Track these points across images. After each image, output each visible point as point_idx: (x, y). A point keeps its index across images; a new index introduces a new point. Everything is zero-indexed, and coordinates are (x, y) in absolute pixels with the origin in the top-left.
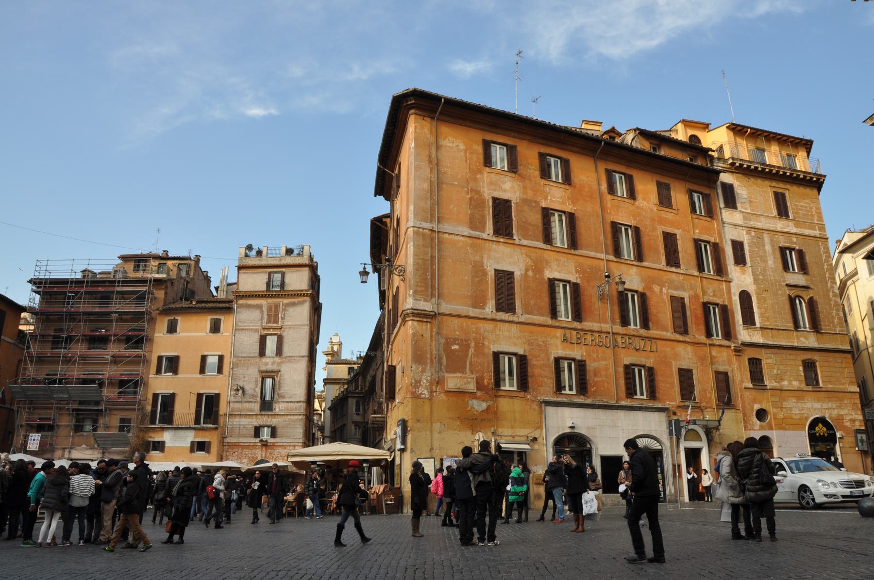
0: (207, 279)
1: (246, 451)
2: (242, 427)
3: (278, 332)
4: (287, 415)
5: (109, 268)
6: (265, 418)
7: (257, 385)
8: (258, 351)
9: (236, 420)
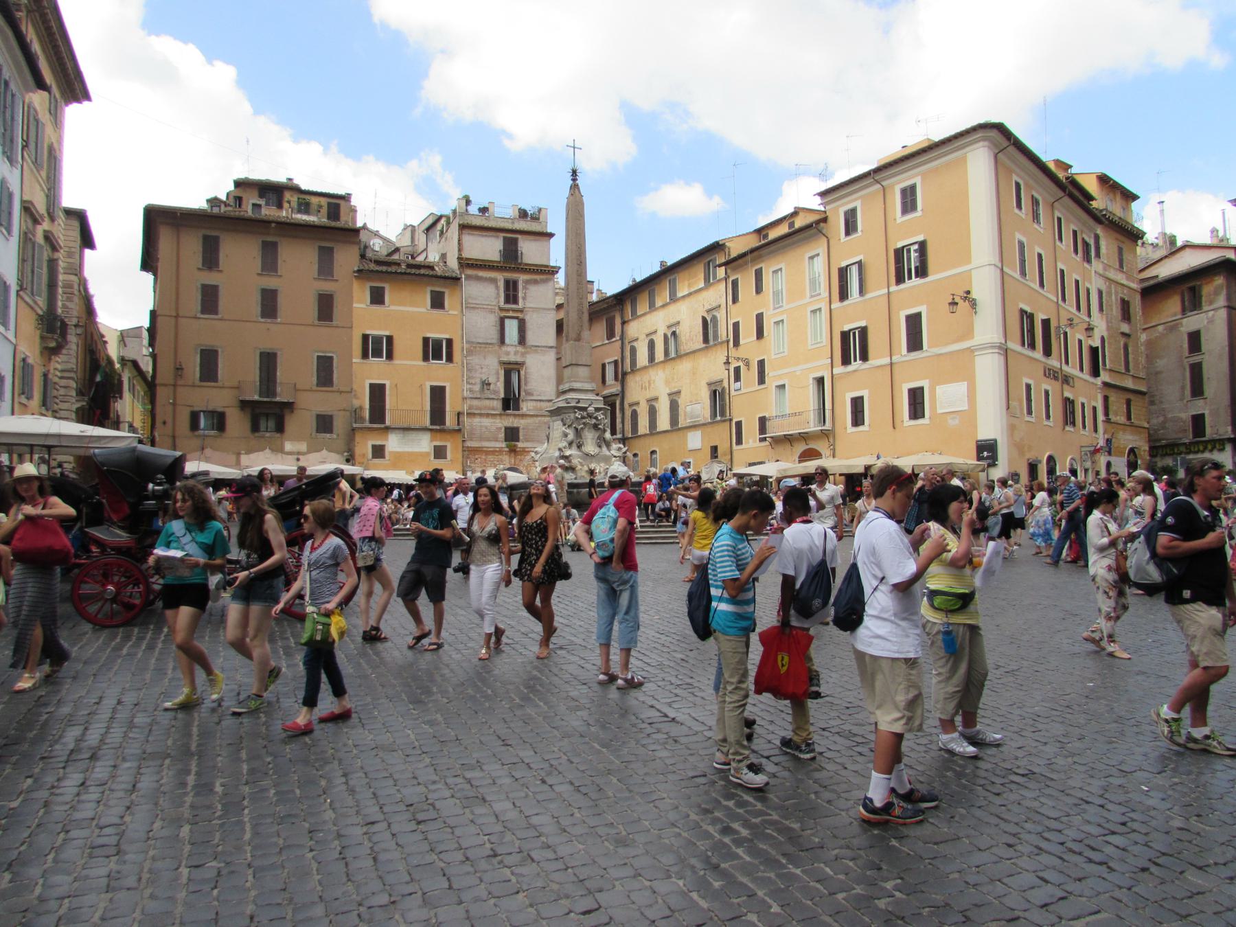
1: (490, 457)
4: (537, 416)
6: (511, 419)
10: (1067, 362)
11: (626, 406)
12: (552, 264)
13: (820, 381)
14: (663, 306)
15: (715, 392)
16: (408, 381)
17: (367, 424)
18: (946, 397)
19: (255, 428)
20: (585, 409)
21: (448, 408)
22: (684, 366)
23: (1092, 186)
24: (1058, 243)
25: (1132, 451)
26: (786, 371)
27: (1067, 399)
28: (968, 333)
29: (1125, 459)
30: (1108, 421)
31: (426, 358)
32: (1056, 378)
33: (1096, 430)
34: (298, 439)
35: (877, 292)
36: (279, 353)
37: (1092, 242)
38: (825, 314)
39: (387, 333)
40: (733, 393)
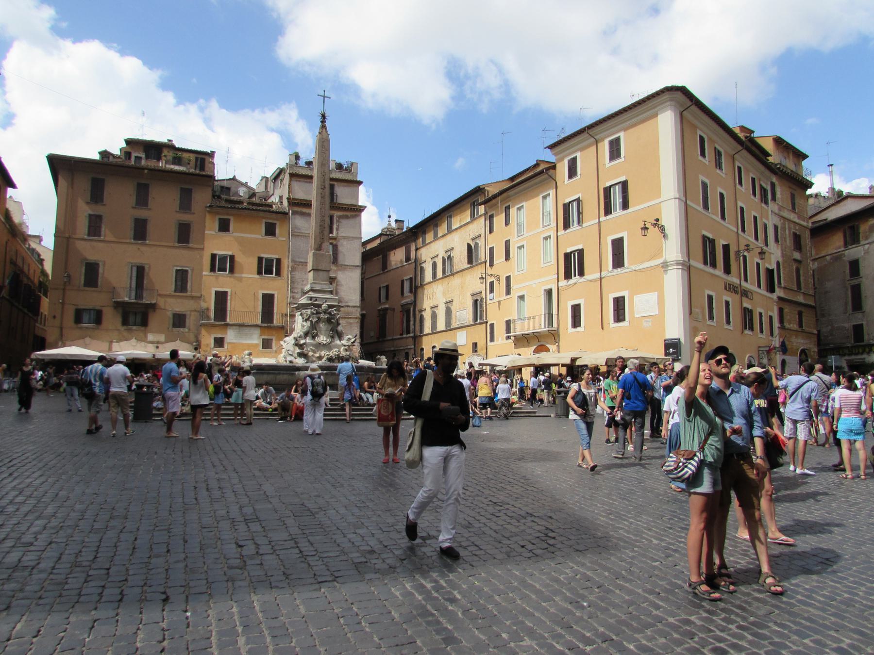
10: (746, 280)
11: (417, 312)
12: (360, 204)
13: (549, 292)
14: (443, 236)
15: (476, 301)
16: (245, 290)
17: (212, 321)
18: (640, 305)
19: (125, 322)
20: (320, 306)
21: (275, 311)
22: (456, 281)
23: (768, 145)
24: (738, 186)
25: (803, 351)
26: (525, 284)
27: (745, 309)
28: (659, 253)
29: (797, 358)
30: (782, 327)
31: (259, 272)
32: (736, 292)
33: (772, 334)
34: (158, 331)
35: (590, 221)
36: (146, 267)
37: (769, 188)
38: (553, 240)
39: (230, 253)
40: (488, 302)
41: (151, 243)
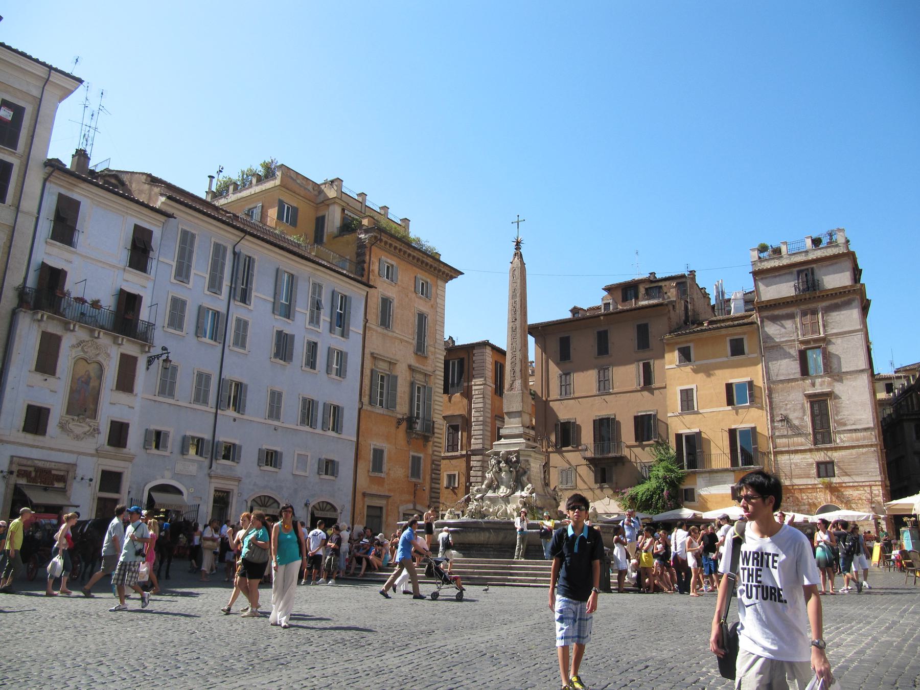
0: (706, 296)
2: (793, 466)
3: (823, 345)
5: (598, 303)
7: (804, 413)
8: (798, 370)
9: (783, 459)
41: (616, 390)
